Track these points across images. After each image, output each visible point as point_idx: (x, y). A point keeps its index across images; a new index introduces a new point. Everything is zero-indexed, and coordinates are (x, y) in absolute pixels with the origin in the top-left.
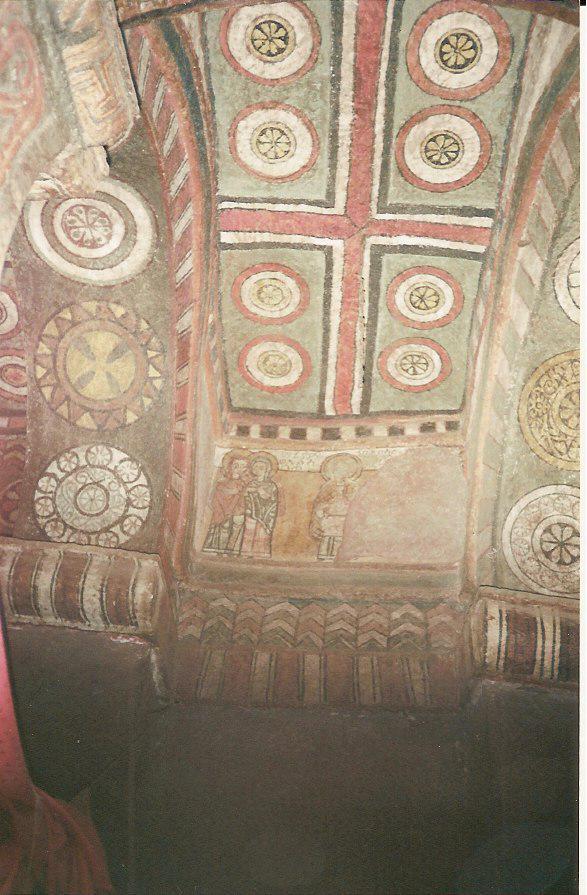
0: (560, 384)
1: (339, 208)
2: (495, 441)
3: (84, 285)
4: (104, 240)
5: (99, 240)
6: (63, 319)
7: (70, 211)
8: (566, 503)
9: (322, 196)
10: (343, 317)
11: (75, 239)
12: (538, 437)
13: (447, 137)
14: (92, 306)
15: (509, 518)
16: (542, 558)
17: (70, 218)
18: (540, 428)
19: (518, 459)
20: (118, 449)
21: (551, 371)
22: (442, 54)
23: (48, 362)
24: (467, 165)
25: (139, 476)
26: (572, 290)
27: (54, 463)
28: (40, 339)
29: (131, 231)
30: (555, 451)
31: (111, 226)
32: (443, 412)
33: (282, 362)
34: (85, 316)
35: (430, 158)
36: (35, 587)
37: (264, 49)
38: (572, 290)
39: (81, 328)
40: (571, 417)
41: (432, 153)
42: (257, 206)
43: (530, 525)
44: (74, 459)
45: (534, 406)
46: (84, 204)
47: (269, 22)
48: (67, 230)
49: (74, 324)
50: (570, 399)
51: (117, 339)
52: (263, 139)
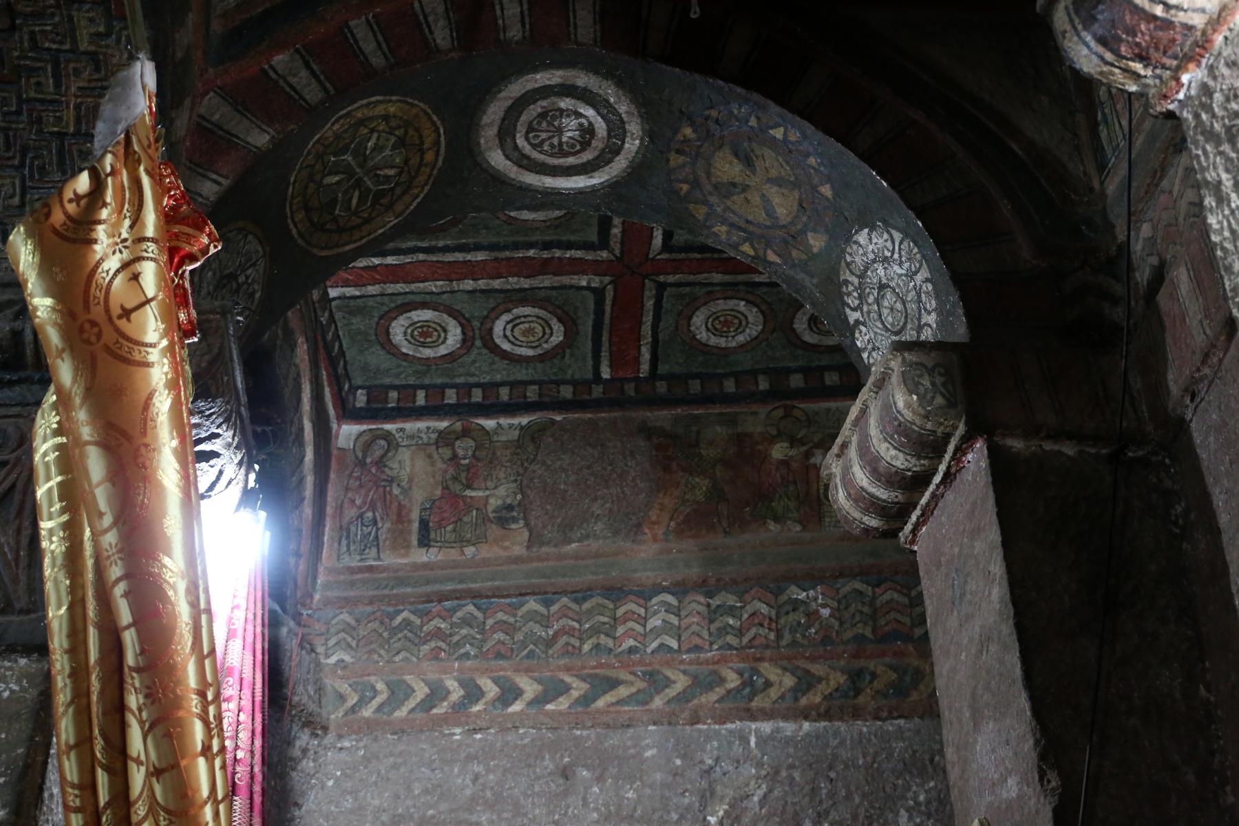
3: (644, 155)
4: (583, 120)
5: (581, 125)
6: (689, 192)
7: (534, 146)
11: (578, 147)
14: (675, 160)
20: (857, 232)
25: (891, 236)
27: (848, 311)
31: (561, 111)
36: (862, 488)
44: (851, 288)
46: (524, 131)
49: (696, 184)
51: (727, 151)
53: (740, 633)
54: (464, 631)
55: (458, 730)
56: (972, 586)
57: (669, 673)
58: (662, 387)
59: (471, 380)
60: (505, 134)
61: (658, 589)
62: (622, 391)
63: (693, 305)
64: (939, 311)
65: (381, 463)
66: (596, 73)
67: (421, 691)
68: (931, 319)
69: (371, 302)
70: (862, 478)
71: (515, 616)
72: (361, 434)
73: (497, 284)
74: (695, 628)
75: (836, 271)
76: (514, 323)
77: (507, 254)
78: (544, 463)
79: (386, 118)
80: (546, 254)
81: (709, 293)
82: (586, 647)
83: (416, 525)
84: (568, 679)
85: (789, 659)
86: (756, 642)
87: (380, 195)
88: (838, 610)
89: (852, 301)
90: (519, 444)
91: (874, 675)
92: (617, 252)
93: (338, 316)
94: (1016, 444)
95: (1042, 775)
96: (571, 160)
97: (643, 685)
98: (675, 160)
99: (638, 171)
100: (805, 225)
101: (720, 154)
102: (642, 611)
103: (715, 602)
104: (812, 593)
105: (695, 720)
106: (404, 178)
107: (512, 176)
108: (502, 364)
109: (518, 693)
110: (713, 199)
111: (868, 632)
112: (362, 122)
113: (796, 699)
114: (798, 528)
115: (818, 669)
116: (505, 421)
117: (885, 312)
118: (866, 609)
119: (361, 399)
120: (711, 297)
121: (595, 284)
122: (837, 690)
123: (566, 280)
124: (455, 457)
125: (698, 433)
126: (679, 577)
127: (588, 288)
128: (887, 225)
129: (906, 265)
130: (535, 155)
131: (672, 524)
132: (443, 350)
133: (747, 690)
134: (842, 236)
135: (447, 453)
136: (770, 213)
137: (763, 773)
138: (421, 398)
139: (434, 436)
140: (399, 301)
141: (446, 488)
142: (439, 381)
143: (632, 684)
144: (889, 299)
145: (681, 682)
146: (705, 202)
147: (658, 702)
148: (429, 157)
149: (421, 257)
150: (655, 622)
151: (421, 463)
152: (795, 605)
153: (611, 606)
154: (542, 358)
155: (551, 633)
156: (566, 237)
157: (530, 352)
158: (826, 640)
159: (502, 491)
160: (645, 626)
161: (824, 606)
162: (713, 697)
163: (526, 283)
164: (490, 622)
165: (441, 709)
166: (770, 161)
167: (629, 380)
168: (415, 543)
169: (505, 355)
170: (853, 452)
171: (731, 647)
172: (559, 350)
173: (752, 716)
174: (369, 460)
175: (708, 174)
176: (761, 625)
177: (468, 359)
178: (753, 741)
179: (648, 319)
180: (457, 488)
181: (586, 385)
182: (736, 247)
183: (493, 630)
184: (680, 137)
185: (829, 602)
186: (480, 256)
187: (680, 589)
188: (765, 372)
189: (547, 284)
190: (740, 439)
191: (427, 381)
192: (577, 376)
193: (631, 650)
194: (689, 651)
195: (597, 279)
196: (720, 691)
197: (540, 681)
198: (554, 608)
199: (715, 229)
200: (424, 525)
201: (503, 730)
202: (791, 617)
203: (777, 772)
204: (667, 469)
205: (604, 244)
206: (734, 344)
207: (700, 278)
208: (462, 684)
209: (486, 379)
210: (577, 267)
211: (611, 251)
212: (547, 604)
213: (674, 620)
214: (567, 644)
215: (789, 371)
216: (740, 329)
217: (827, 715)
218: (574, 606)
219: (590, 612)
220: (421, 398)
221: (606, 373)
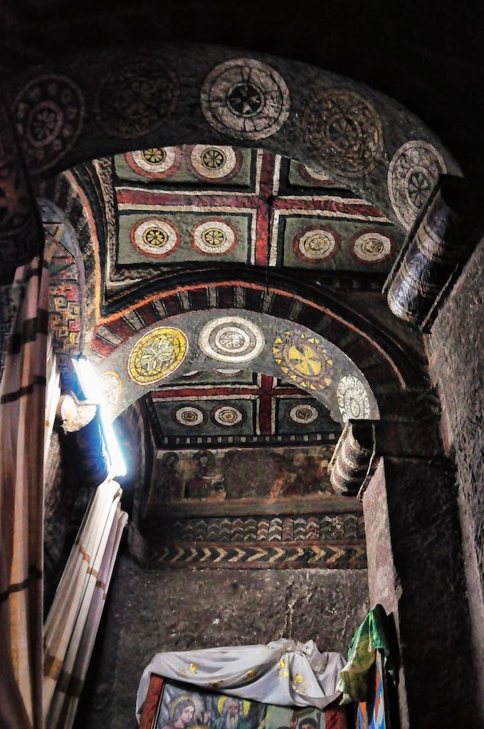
1: (254, 212)
7: (223, 345)
8: (400, 169)
9: (246, 218)
10: (335, 209)
13: (205, 157)
14: (275, 351)
17: (227, 345)
22: (156, 162)
23: (299, 380)
28: (289, 376)
29: (234, 325)
31: (232, 332)
33: (371, 244)
34: (280, 354)
35: (219, 165)
37: (162, 240)
38: (257, 129)
39: (286, 358)
41: (215, 164)
42: (253, 247)
47: (147, 238)
48: (233, 347)
49: (283, 360)
52: (211, 242)
53: (305, 534)
54: (200, 530)
55: (195, 568)
56: (378, 514)
57: (276, 549)
58: (280, 438)
59: (207, 434)
60: (211, 341)
61: (274, 516)
62: (264, 439)
63: (290, 407)
64: (371, 408)
65: (172, 465)
66: (244, 318)
67: (182, 552)
68: (368, 411)
69: (168, 404)
70: (340, 473)
71: (219, 525)
72: (165, 454)
73: (215, 398)
74: (288, 532)
75: (335, 394)
76: (223, 413)
77: (219, 386)
78: (234, 467)
79: (165, 335)
80: (233, 387)
81: (296, 402)
82: (246, 538)
83: (184, 489)
84: (237, 550)
85: (324, 545)
86: (312, 538)
87: (165, 362)
88: (344, 526)
89: (342, 405)
90: (224, 459)
91: (356, 551)
92: (260, 386)
93: (157, 409)
94: (395, 460)
95: (396, 587)
96: (237, 351)
97: (266, 553)
98: (275, 351)
99: (262, 355)
100: (324, 375)
101: (292, 348)
102: (268, 525)
103: (297, 522)
104: (334, 519)
105: (286, 567)
106: (174, 356)
107: (215, 356)
108: (218, 429)
109: (217, 555)
110: (290, 365)
111: (355, 535)
112: (156, 336)
113: (325, 560)
114: (330, 494)
115: (334, 549)
116: (219, 450)
117: (353, 408)
118: (355, 526)
119: (166, 440)
120: (297, 404)
121: (253, 397)
122: (341, 557)
123: (242, 396)
124: (200, 463)
125: (293, 456)
126: (282, 512)
127: (250, 400)
128: (352, 375)
129: (359, 391)
130: (223, 349)
131: (282, 491)
132: (196, 423)
133: (306, 557)
134: (336, 379)
135: (197, 462)
136: (311, 371)
137: (311, 588)
138: (188, 441)
139: (192, 456)
140: (179, 403)
141: (196, 476)
142: (195, 434)
143: (262, 553)
144: (354, 403)
145: (281, 553)
146: (288, 367)
147: (272, 560)
148: (183, 349)
149: (187, 387)
150: (272, 529)
151: (187, 464)
152: (328, 523)
153: (256, 522)
154: (235, 426)
155: (232, 532)
156: (240, 380)
157: (229, 424)
158: (339, 538)
159: (217, 477)
160: (268, 530)
161: (339, 524)
162: (293, 558)
163: (226, 397)
164: (209, 527)
165: (189, 559)
166: (309, 352)
167: (267, 436)
168: (183, 496)
169: (220, 425)
170: (337, 462)
171: (302, 540)
172: (241, 424)
173: (308, 566)
174: (168, 464)
175: (288, 357)
176: (314, 531)
177: (206, 427)
178: (308, 577)
179: (274, 412)
180: (200, 475)
181: (251, 437)
182: (299, 383)
183: (210, 530)
184: (276, 342)
185: (341, 523)
186: (209, 387)
187: (283, 516)
188: (320, 433)
189: (234, 398)
190: (309, 459)
191: (191, 434)
192: (248, 433)
193: (263, 540)
194: (285, 541)
195: (253, 396)
196: (296, 556)
197: (227, 551)
198: (234, 523)
199: (292, 377)
200: (187, 489)
201: (212, 569)
202: (326, 528)
203: (317, 588)
204: (280, 470)
205: (255, 382)
206: (307, 422)
207: (293, 396)
208: (197, 551)
209: (213, 434)
210: (245, 391)
211: (258, 386)
212: (232, 521)
213: (280, 528)
214: (239, 537)
215: (328, 433)
216: (309, 416)
217: (337, 567)
218: (242, 522)
219: (248, 525)
220: (188, 441)
221: (258, 432)
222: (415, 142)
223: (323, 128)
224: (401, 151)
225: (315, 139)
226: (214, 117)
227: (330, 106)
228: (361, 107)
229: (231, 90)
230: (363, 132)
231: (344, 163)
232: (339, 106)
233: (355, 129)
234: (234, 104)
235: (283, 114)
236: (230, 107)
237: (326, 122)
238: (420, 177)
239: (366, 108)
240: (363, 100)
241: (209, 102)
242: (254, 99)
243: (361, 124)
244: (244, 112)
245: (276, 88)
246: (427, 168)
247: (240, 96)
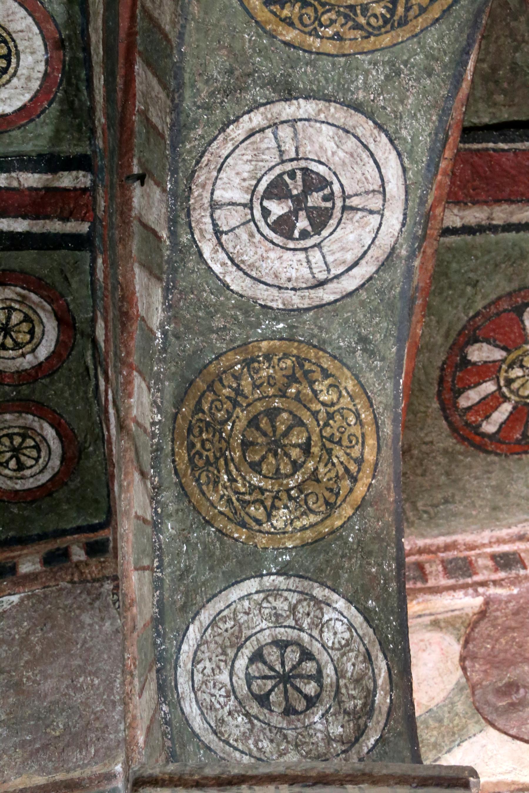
0: (235, 404)
2: (145, 521)
8: (282, 606)
12: (214, 498)
15: (185, 647)
16: (254, 708)
18: (216, 483)
19: (187, 541)
21: (218, 385)
24: (29, 79)
26: (224, 237)
30: (247, 519)
32: (79, 530)
38: (224, 237)
40: (264, 458)
43: (224, 653)
45: (198, 446)
50: (258, 428)
222: (360, 619)
223: (271, 391)
224: (319, 592)
225: (237, 378)
226: (252, 134)
227: (324, 397)
228: (353, 468)
229: (321, 169)
230: (300, 488)
231: (208, 463)
232: (330, 416)
233: (296, 466)
234: (286, 177)
235: (274, 292)
236: (277, 171)
237: (283, 395)
238: (309, 667)
239: (355, 480)
240: (367, 470)
241: (293, 122)
242: (303, 223)
243: (314, 477)
244: (266, 203)
245: (334, 272)
246: (339, 673)
247: (308, 189)
